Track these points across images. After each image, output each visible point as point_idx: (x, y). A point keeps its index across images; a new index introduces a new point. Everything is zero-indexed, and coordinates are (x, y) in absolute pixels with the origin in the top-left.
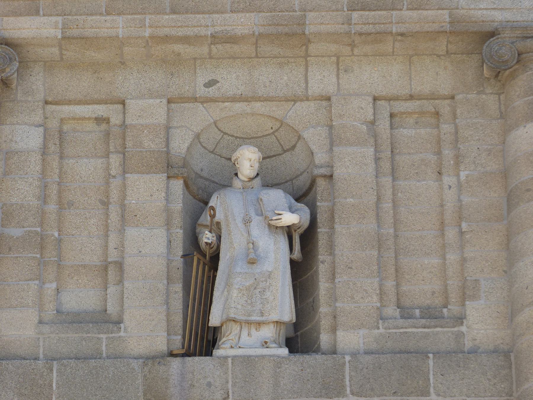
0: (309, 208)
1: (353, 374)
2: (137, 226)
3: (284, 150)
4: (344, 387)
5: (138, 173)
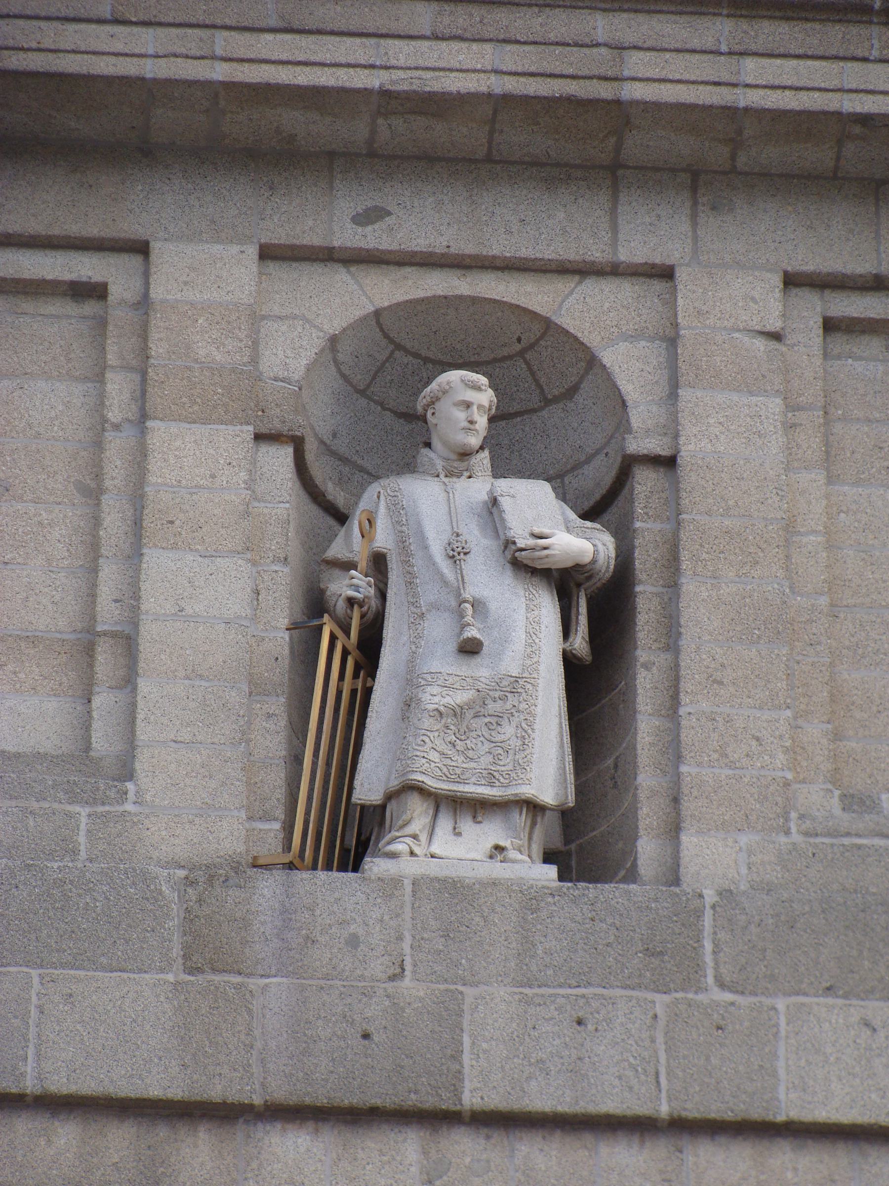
0: (615, 534)
1: (722, 935)
2: (175, 547)
3: (546, 398)
4: (699, 967)
5: (180, 419)
